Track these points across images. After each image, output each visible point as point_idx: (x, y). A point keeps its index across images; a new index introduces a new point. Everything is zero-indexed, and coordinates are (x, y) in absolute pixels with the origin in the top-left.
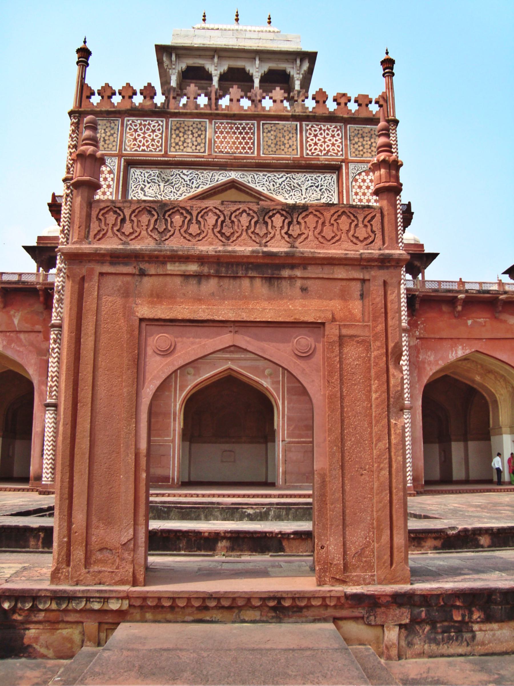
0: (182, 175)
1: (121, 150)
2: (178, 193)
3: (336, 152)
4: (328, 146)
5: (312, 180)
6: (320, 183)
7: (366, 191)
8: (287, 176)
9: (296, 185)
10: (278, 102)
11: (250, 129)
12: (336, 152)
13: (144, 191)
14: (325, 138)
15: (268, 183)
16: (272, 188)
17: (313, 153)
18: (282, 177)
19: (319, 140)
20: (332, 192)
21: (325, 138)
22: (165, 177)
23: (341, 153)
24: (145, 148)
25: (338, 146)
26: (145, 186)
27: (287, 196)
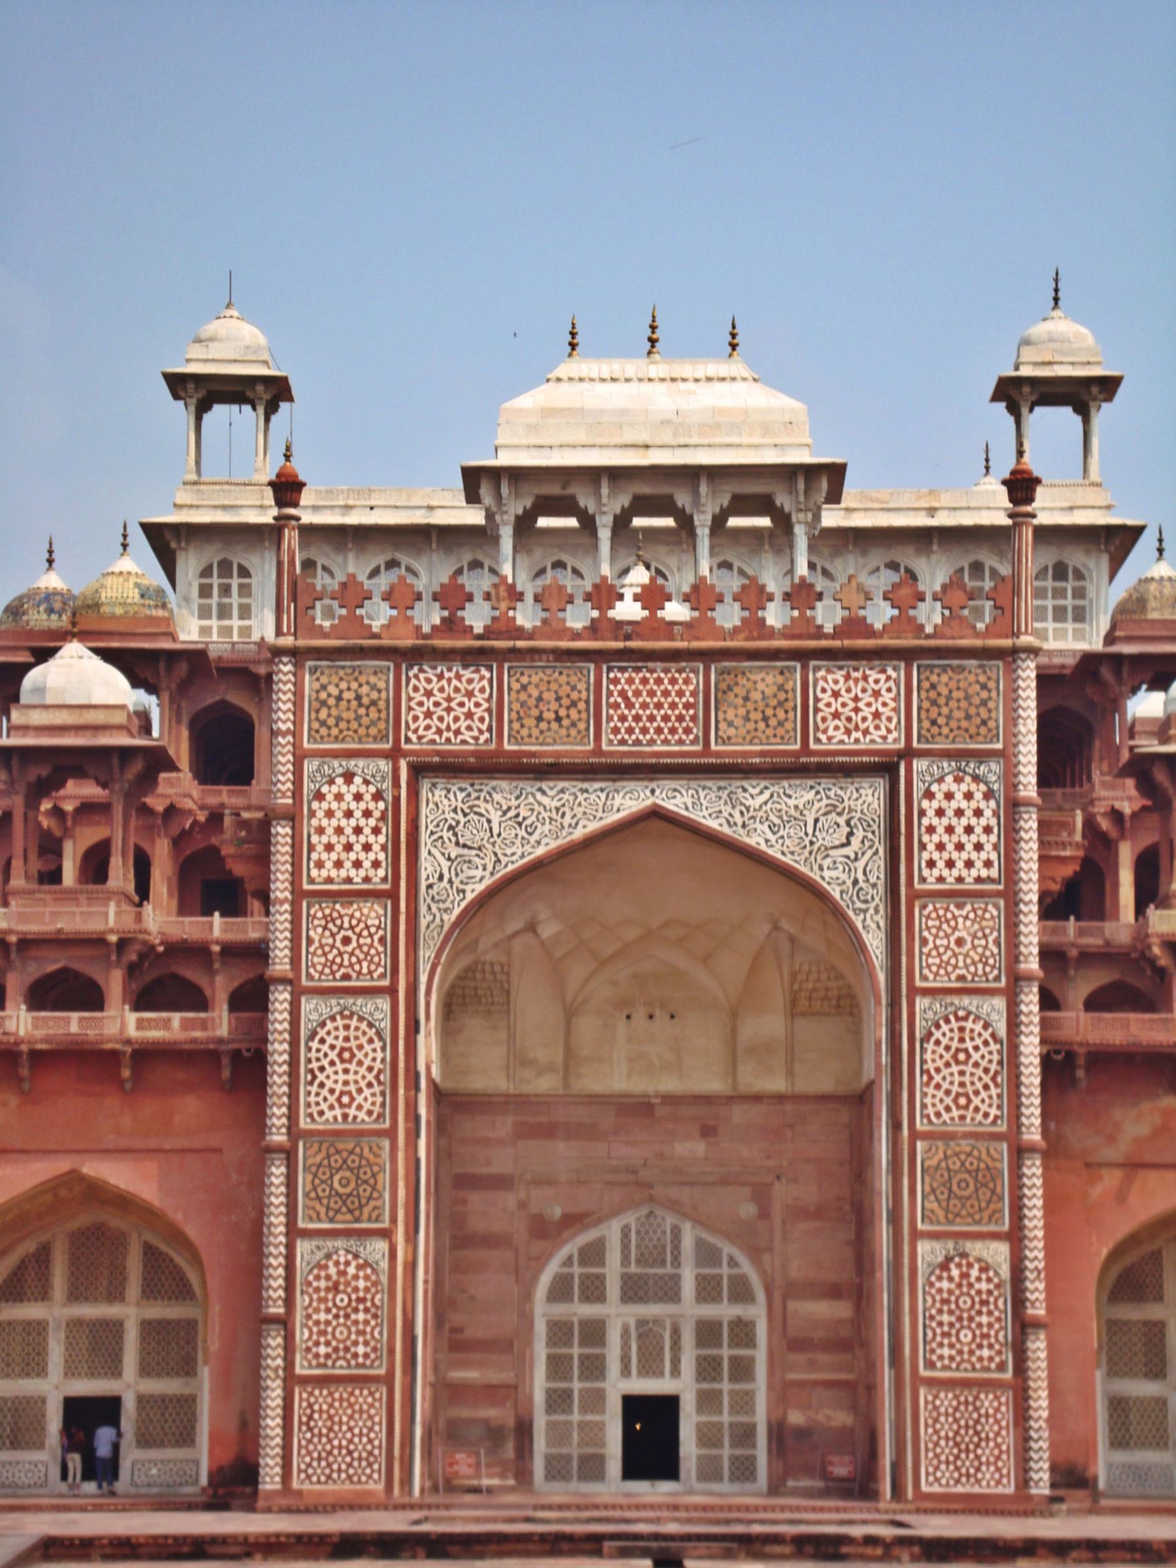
0: (539, 796)
1: (397, 741)
2: (533, 839)
3: (883, 732)
4: (864, 719)
5: (828, 797)
6: (846, 803)
7: (954, 821)
8: (772, 789)
9: (792, 812)
10: (754, 607)
11: (687, 681)
12: (883, 732)
13: (455, 834)
14: (856, 699)
15: (729, 808)
16: (739, 819)
17: (830, 739)
18: (761, 792)
19: (844, 705)
20: (875, 827)
21: (856, 699)
22: (503, 802)
23: (895, 734)
24: (451, 735)
25: (889, 719)
26: (458, 823)
27: (773, 838)
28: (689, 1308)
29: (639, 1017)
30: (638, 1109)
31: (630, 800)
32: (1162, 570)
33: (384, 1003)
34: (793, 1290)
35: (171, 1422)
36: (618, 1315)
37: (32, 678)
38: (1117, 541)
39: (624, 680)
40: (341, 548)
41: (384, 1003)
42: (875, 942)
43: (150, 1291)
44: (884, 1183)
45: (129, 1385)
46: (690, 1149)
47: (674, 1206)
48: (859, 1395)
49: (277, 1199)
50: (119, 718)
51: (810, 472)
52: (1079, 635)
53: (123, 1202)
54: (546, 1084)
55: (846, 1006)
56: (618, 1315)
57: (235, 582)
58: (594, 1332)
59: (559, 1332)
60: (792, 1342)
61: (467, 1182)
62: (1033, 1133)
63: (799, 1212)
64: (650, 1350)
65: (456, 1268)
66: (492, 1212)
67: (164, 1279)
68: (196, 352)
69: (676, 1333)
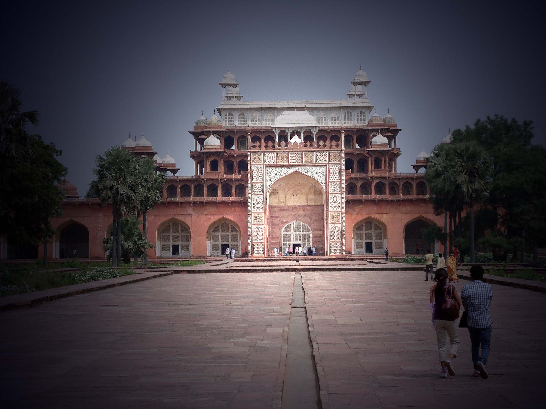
28: (302, 233)
29: (295, 196)
30: (295, 207)
31: (293, 170)
32: (376, 114)
33: (262, 196)
34: (315, 230)
35: (236, 247)
36: (292, 234)
37: (206, 140)
38: (370, 108)
39: (293, 154)
40: (248, 111)
41: (262, 196)
42: (324, 187)
43: (232, 231)
44: (325, 217)
45: (230, 243)
46: (302, 212)
47: (299, 220)
48: (323, 243)
49: (250, 220)
50: (219, 147)
51: (315, 127)
52: (364, 123)
53: (229, 220)
54: (283, 204)
55: (321, 193)
56: (292, 234)
57: (231, 116)
58: (289, 236)
59: (285, 236)
60: (315, 237)
61: (272, 217)
62: (344, 211)
63: (316, 220)
64: (297, 238)
65: (272, 228)
66: (276, 221)
67: (234, 229)
68: (224, 79)
69: (300, 236)
